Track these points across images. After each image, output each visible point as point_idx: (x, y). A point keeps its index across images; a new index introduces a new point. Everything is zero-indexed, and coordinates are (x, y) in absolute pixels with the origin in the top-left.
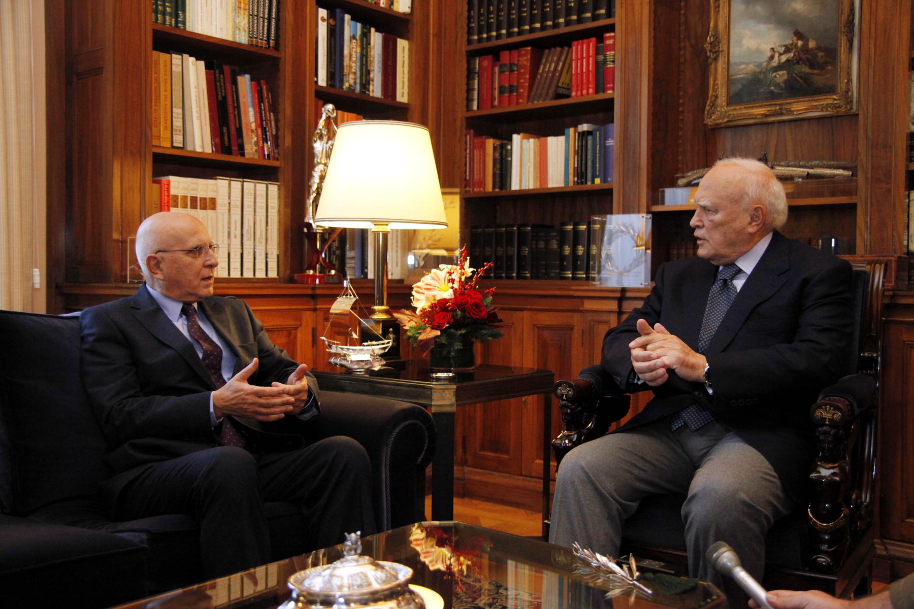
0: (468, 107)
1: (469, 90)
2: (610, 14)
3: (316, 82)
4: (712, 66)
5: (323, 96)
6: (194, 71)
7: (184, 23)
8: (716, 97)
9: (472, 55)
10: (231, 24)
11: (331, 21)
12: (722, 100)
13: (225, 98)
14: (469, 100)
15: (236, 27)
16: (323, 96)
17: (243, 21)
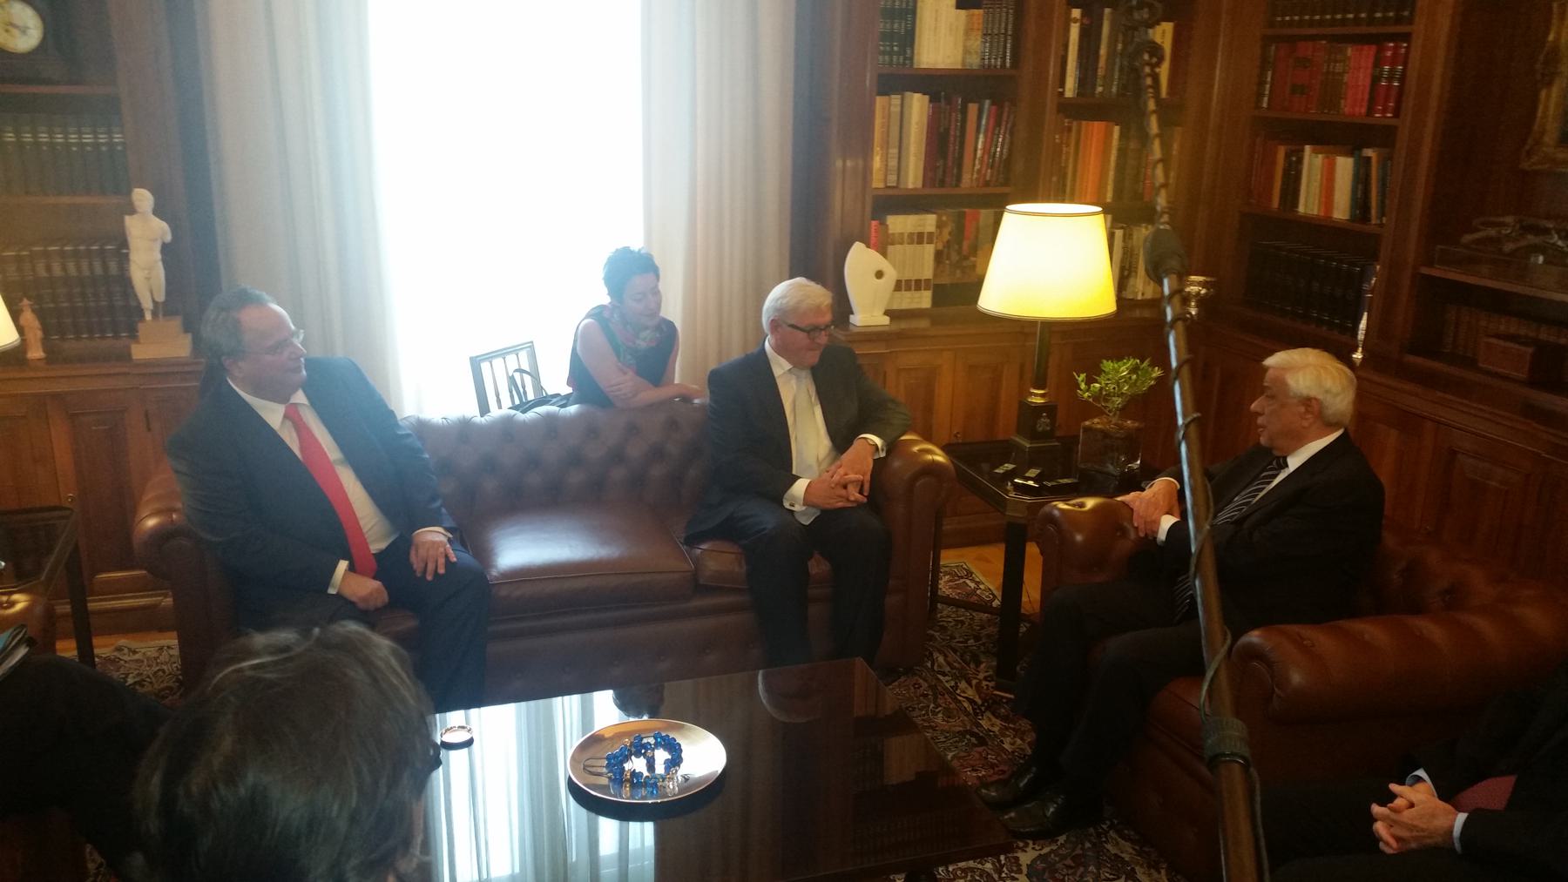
0: (1258, 106)
1: (1261, 83)
2: (1410, 21)
3: (1062, 94)
4: (1543, 94)
5: (1070, 110)
6: (918, 105)
7: (911, 59)
8: (1543, 133)
9: (1267, 40)
10: (961, 49)
11: (1086, 21)
12: (1551, 137)
13: (947, 131)
14: (1260, 95)
15: (966, 51)
16: (1070, 110)
17: (976, 43)
